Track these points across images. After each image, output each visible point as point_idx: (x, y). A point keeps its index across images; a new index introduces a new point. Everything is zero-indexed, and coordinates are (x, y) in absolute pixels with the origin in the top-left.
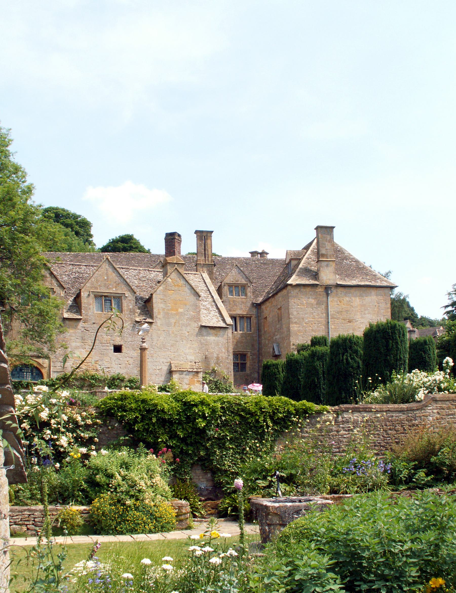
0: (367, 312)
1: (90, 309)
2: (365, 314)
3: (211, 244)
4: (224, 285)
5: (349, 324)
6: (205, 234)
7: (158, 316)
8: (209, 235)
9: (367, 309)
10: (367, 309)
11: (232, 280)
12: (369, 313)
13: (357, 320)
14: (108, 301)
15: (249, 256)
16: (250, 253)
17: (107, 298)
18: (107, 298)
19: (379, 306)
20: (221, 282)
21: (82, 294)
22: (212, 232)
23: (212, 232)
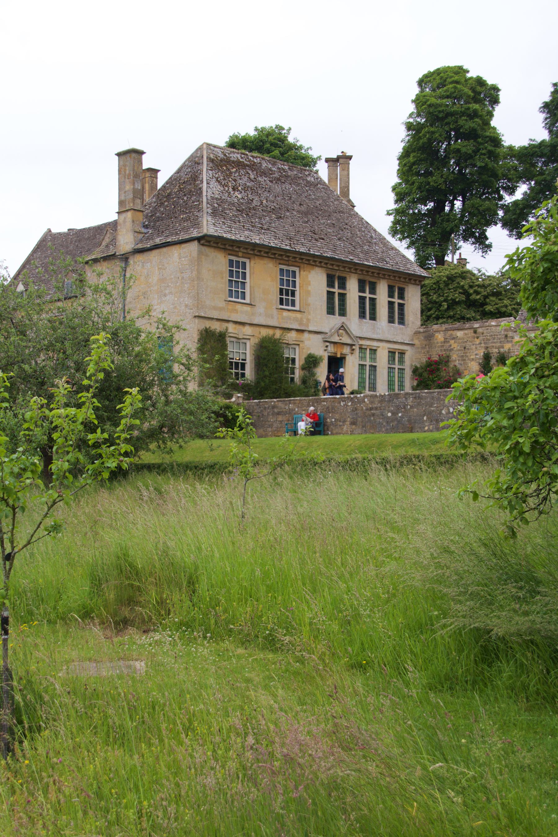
0: (167, 292)
2: (165, 295)
12: (171, 293)
13: (155, 307)
19: (183, 278)
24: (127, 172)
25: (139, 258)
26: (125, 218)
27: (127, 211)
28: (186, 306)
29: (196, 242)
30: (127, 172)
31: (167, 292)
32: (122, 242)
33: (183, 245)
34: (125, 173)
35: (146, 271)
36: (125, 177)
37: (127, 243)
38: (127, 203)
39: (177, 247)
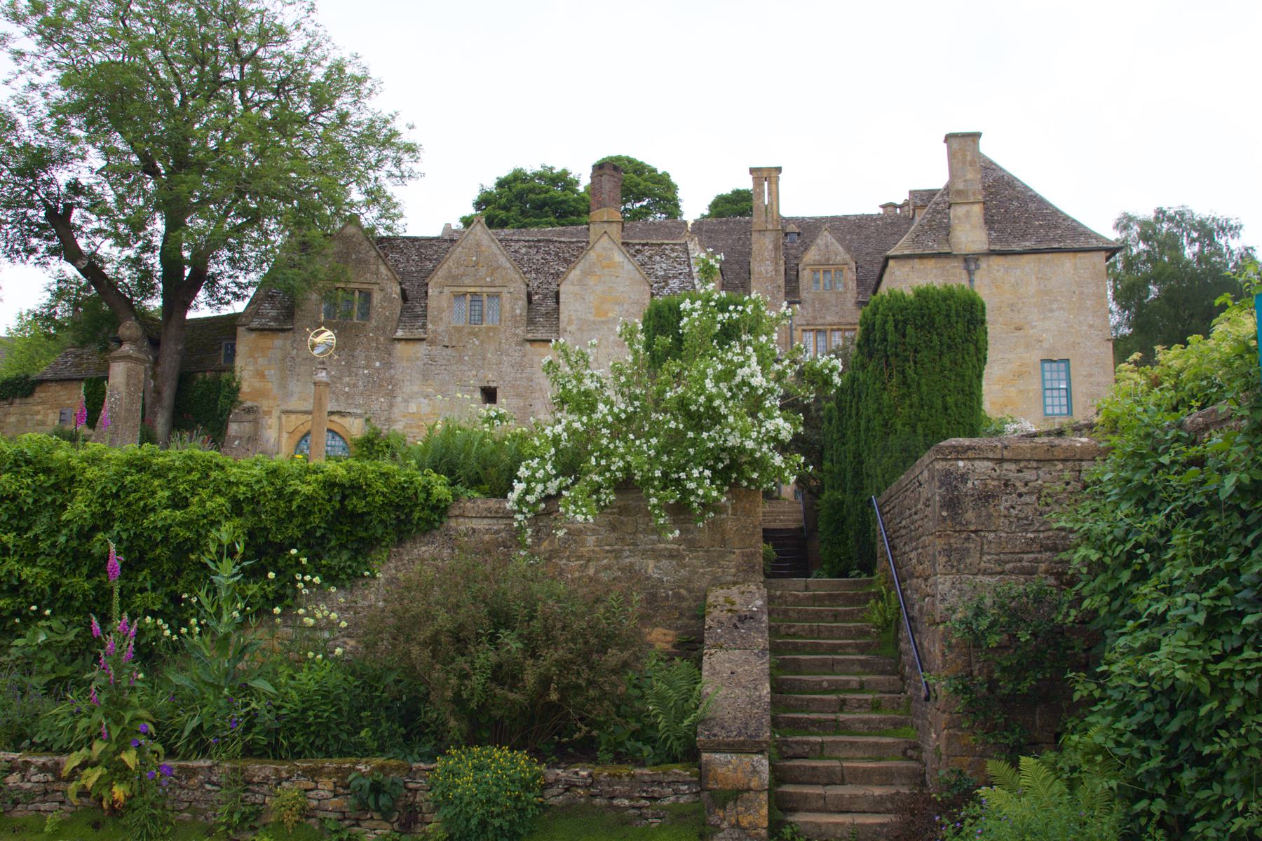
0: (1054, 307)
1: (441, 319)
2: (1051, 311)
3: (778, 192)
4: (804, 269)
5: (1017, 333)
6: (765, 175)
7: (569, 328)
8: (773, 175)
9: (1056, 300)
10: (1056, 300)
11: (817, 258)
12: (1061, 309)
13: (1034, 324)
14: (477, 303)
15: (881, 211)
16: (883, 207)
17: (476, 298)
18: (476, 298)
19: (1082, 293)
20: (798, 265)
21: (430, 291)
22: (779, 170)
23: (779, 170)
24: (969, 158)
25: (996, 261)
26: (968, 212)
27: (973, 203)
28: (1091, 326)
29: (1103, 255)
30: (969, 158)
31: (1054, 307)
32: (963, 239)
33: (1080, 255)
34: (964, 157)
35: (1013, 280)
36: (964, 163)
37: (973, 242)
38: (970, 194)
39: (1071, 255)
